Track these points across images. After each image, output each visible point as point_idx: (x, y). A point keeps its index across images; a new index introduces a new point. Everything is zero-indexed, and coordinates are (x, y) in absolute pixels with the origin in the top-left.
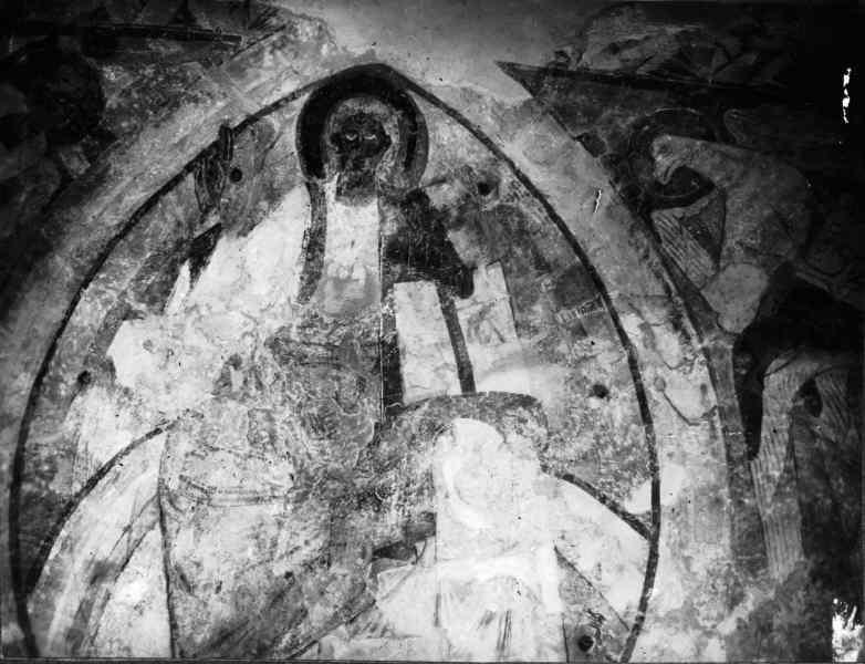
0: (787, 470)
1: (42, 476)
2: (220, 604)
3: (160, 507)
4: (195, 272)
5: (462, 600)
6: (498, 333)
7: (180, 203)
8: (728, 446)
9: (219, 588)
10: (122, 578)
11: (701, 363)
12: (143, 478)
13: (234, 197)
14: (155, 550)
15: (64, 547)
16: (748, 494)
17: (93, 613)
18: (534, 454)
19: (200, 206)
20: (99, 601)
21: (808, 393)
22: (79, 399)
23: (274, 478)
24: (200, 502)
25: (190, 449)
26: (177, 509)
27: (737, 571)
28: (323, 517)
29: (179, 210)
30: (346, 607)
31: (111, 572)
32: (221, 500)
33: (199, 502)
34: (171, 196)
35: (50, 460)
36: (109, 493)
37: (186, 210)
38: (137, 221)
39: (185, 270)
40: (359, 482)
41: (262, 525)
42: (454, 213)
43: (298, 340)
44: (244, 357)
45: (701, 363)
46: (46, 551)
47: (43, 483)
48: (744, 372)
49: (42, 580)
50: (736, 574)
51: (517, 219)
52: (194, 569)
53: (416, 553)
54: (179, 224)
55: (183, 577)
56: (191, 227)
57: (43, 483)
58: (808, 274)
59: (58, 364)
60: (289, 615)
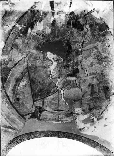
1: (6, 64)
2: (40, 85)
3: (28, 69)
4: (32, 29)
5: (84, 83)
6: (88, 37)
7: (28, 16)
9: (39, 83)
10: (22, 81)
12: (24, 64)
13: (38, 15)
14: (27, 76)
15: (11, 76)
17: (17, 87)
18: (96, 58)
19: (32, 17)
20: (18, 85)
22: (11, 51)
23: (49, 64)
24: (35, 68)
25: (33, 59)
26: (31, 69)
28: (58, 70)
29: (28, 18)
30: (63, 85)
31: (20, 80)
32: (39, 68)
33: (35, 68)
34: (26, 15)
35: (7, 61)
36: (18, 67)
37: (29, 18)
38: (20, 19)
39: (30, 28)
40: (64, 64)
41: (46, 72)
42: (79, 16)
43: (51, 40)
44: (42, 43)
46: (7, 77)
47: (6, 65)
49: (7, 81)
51: (91, 16)
52: (35, 79)
53: (75, 75)
54: (28, 20)
55: (33, 81)
56: (30, 21)
57: (6, 65)
59: (7, 45)
60: (53, 87)
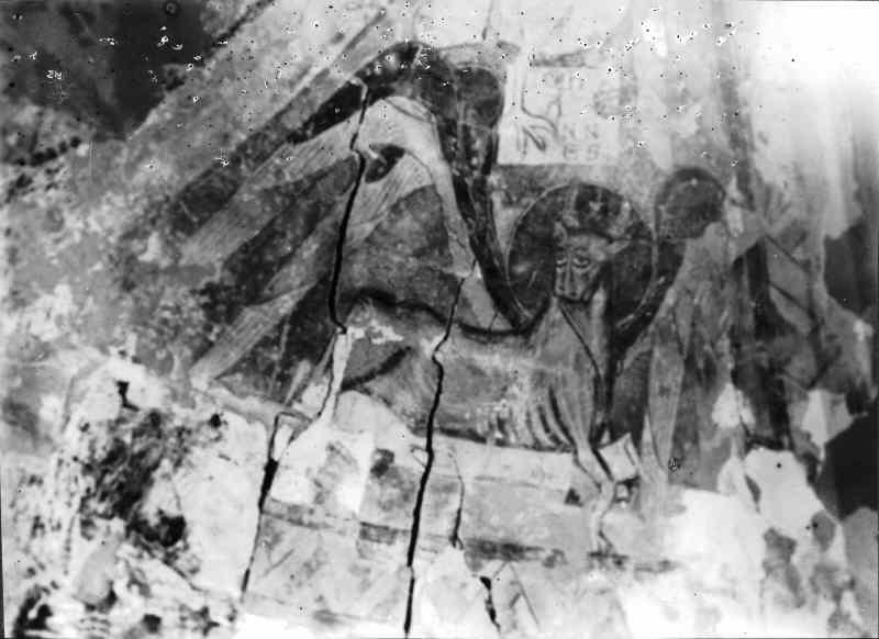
0: (297, 184)
8: (290, 106)
11: (366, 17)
16: (251, 163)
21: (387, 158)
27: (167, 210)
45: (366, 17)
48: (377, 70)
50: (163, 213)
58: (515, 81)
